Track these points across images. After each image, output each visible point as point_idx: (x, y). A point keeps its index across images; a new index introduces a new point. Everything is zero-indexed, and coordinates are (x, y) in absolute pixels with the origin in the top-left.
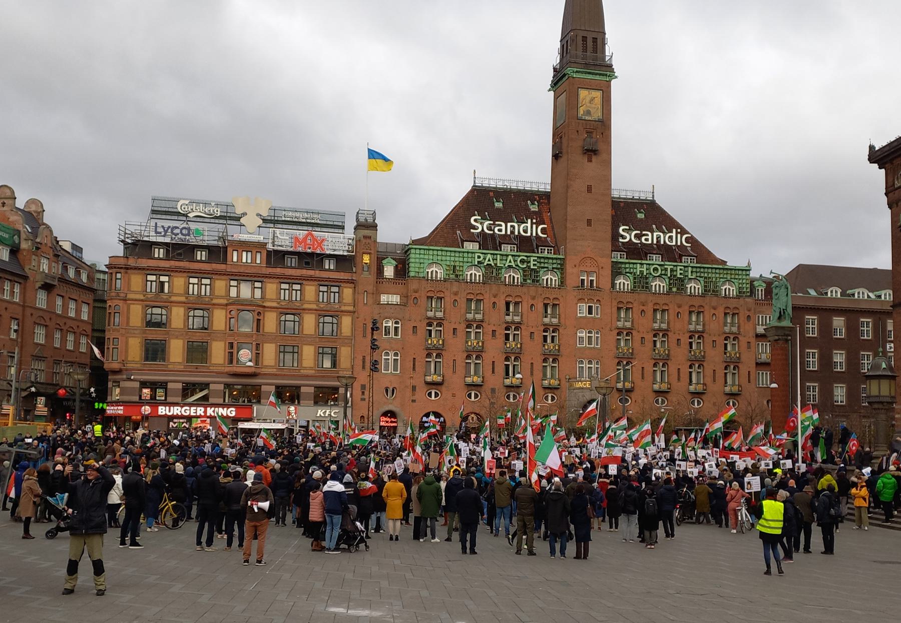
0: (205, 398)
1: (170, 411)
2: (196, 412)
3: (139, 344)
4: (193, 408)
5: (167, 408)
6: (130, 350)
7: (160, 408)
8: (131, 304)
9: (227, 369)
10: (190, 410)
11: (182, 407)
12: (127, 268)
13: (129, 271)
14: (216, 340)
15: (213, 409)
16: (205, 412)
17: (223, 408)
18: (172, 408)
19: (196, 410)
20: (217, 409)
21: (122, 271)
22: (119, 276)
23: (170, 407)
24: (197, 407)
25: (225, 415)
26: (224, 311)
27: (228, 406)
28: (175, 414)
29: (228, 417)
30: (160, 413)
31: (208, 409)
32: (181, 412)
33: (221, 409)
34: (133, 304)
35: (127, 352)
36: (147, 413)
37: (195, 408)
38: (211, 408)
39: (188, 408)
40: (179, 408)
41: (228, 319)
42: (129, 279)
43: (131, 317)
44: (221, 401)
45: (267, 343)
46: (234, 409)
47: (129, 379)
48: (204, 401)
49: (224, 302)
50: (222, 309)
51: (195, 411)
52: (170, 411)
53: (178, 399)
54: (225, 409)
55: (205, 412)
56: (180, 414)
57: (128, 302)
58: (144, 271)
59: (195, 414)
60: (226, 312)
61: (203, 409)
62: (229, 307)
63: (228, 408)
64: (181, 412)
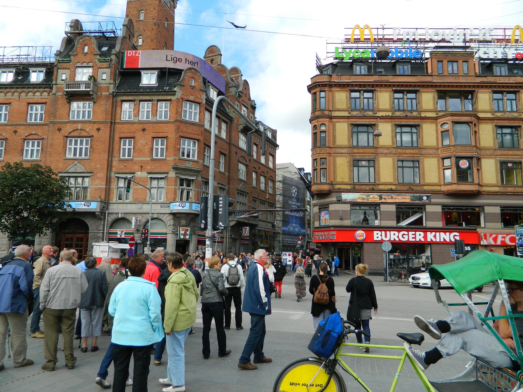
0: (419, 221)
1: (386, 236)
2: (415, 238)
3: (347, 164)
4: (411, 233)
5: (383, 233)
6: (338, 171)
7: (375, 232)
8: (337, 122)
9: (444, 188)
10: (408, 235)
11: (399, 232)
12: (331, 85)
13: (334, 89)
14: (429, 157)
15: (434, 233)
16: (425, 237)
17: (445, 232)
18: (388, 232)
19: (415, 234)
20: (438, 234)
21: (326, 89)
22: (323, 94)
23: (386, 231)
24: (415, 231)
25: (448, 240)
26: (433, 126)
27: (451, 231)
28: (392, 239)
29: (451, 243)
30: (375, 239)
31: (429, 233)
32: (398, 237)
33: (442, 234)
34: (339, 122)
35: (335, 172)
36: (360, 239)
37: (414, 233)
38: (431, 232)
39: (406, 233)
40: (396, 233)
41: (440, 133)
42: (333, 97)
43: (337, 136)
44: (440, 224)
45: (486, 158)
46: (457, 234)
47: (340, 201)
48: (417, 225)
49: (433, 115)
50: (431, 123)
51: (414, 236)
52: (386, 236)
53: (393, 223)
54: (448, 234)
55: (425, 237)
56: (397, 239)
57: (333, 120)
58: (348, 89)
59: (414, 240)
60: (437, 126)
61: (422, 234)
62: (439, 120)
63: (450, 232)
64: (398, 237)
